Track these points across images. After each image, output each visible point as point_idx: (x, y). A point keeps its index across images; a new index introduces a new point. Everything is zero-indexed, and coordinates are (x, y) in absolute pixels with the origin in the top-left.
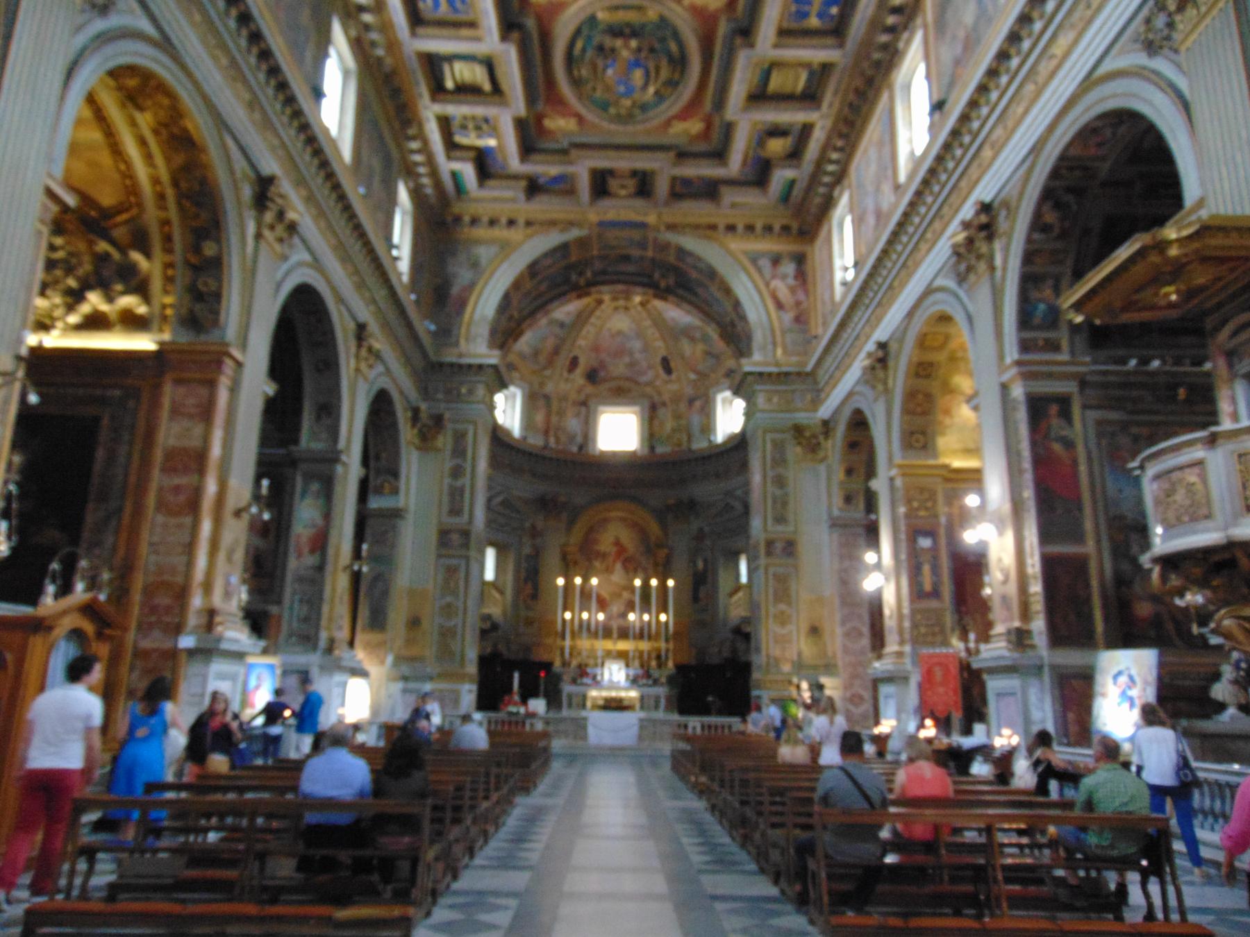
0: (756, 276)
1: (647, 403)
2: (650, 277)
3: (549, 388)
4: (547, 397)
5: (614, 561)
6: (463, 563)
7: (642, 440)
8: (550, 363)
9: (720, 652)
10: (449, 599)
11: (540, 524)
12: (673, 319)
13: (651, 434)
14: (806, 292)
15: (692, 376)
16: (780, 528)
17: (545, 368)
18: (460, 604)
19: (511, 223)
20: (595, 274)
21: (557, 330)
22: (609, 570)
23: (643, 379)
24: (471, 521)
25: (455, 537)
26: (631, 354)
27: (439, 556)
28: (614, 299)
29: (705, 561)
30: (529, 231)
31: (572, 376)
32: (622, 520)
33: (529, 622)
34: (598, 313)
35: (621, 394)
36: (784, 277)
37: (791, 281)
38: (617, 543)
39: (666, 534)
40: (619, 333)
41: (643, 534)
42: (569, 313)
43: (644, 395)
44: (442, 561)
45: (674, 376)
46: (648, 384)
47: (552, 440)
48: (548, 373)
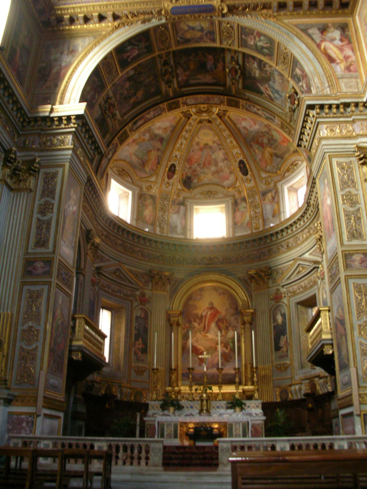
0: (309, 41)
1: (230, 201)
2: (224, 85)
3: (155, 191)
4: (153, 197)
5: (209, 323)
6: (46, 288)
7: (228, 228)
8: (154, 172)
9: (300, 389)
10: (30, 324)
11: (148, 293)
12: (244, 128)
13: (234, 224)
14: (353, 50)
15: (264, 175)
16: (355, 242)
17: (151, 176)
18: (42, 328)
19: (101, 18)
20: (180, 87)
21: (158, 144)
22: (206, 329)
23: (226, 183)
24: (54, 252)
25: (39, 265)
26: (216, 164)
27: (23, 284)
28: (200, 112)
29: (283, 316)
30: (116, 23)
31: (171, 181)
32: (215, 289)
33: (140, 372)
34: (187, 127)
35: (209, 197)
36: (332, 40)
37: (338, 42)
38: (212, 308)
39: (251, 296)
40: (206, 145)
41: (233, 300)
42: (165, 129)
43: (226, 196)
44: (26, 288)
45: (249, 176)
46: (233, 186)
47: (158, 229)
48: (153, 179)
